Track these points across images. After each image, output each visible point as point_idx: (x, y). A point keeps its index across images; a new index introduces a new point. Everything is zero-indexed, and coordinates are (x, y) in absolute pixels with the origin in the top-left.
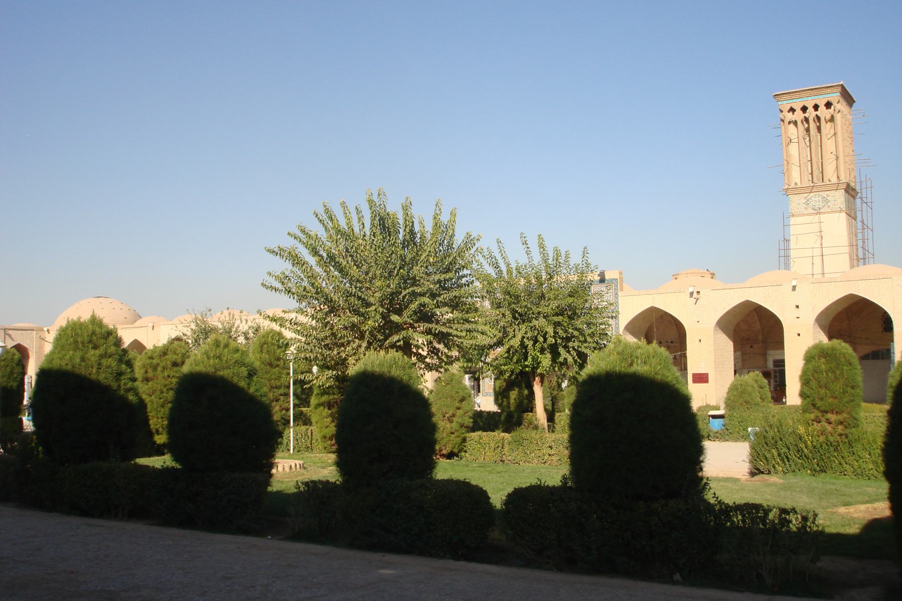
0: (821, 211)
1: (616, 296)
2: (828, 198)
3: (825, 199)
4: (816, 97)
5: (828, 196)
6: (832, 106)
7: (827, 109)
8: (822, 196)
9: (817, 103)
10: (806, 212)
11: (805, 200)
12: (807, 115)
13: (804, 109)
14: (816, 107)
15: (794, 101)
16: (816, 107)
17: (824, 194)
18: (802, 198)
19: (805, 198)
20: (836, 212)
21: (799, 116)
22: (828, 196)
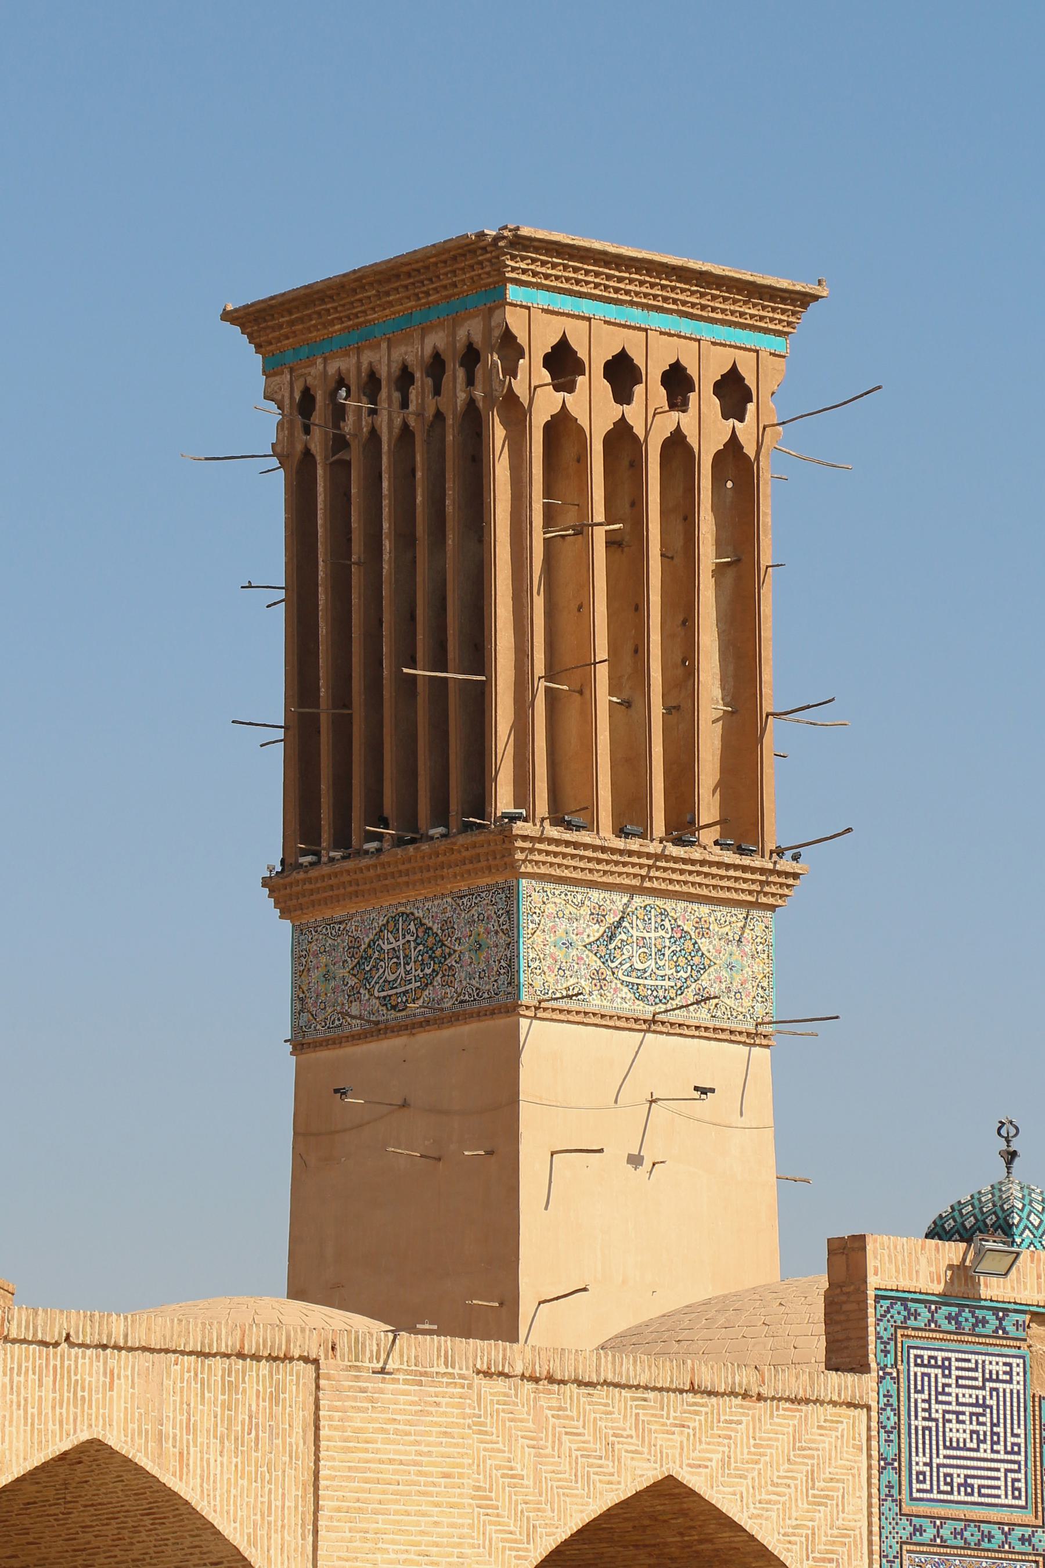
2: (704, 944)
3: (689, 945)
4: (686, 327)
6: (751, 407)
7: (726, 417)
9: (683, 362)
10: (595, 1002)
11: (596, 931)
15: (586, 307)
18: (585, 911)
19: (598, 917)
20: (731, 1036)
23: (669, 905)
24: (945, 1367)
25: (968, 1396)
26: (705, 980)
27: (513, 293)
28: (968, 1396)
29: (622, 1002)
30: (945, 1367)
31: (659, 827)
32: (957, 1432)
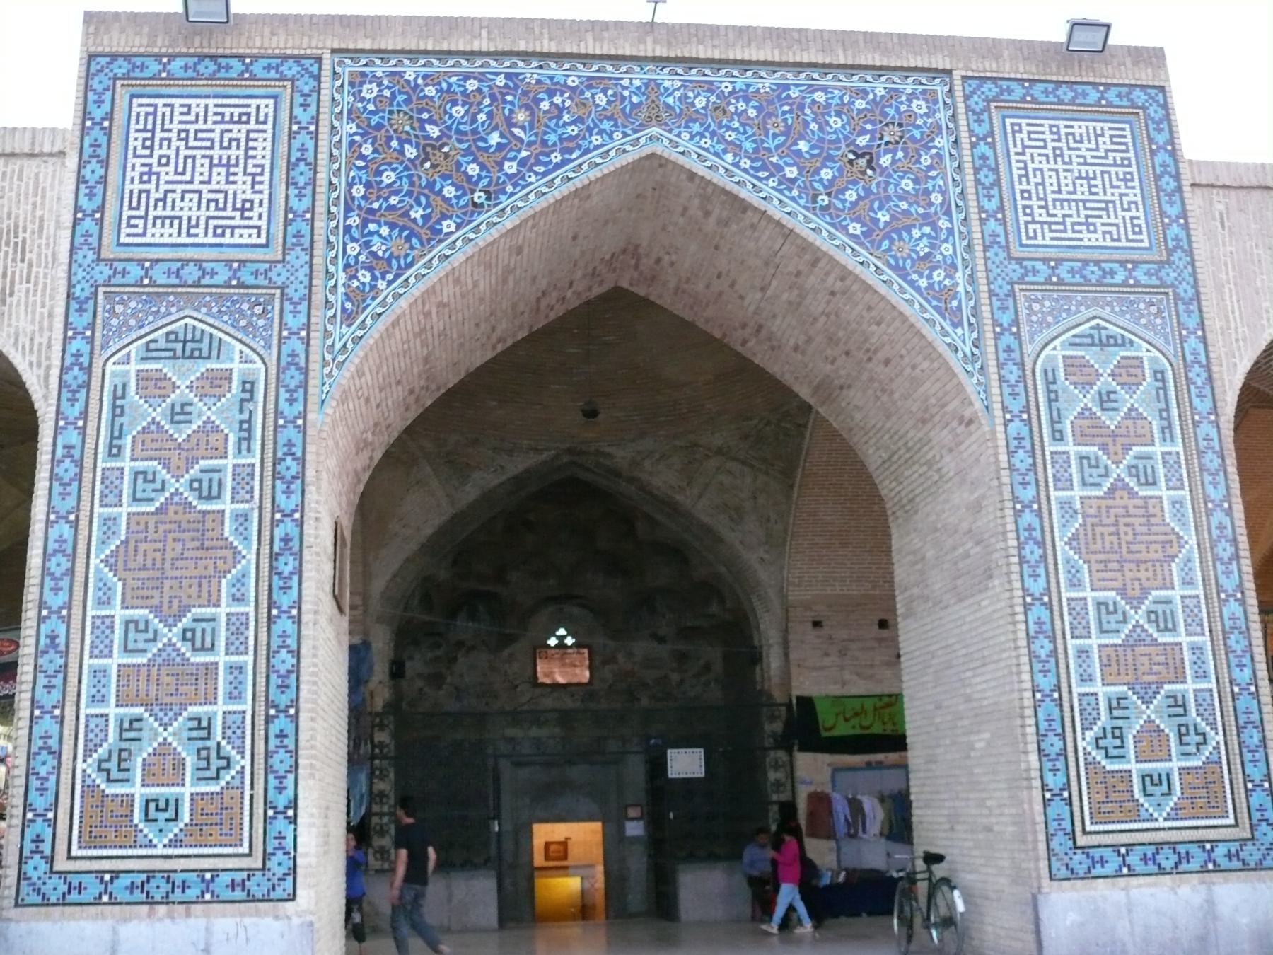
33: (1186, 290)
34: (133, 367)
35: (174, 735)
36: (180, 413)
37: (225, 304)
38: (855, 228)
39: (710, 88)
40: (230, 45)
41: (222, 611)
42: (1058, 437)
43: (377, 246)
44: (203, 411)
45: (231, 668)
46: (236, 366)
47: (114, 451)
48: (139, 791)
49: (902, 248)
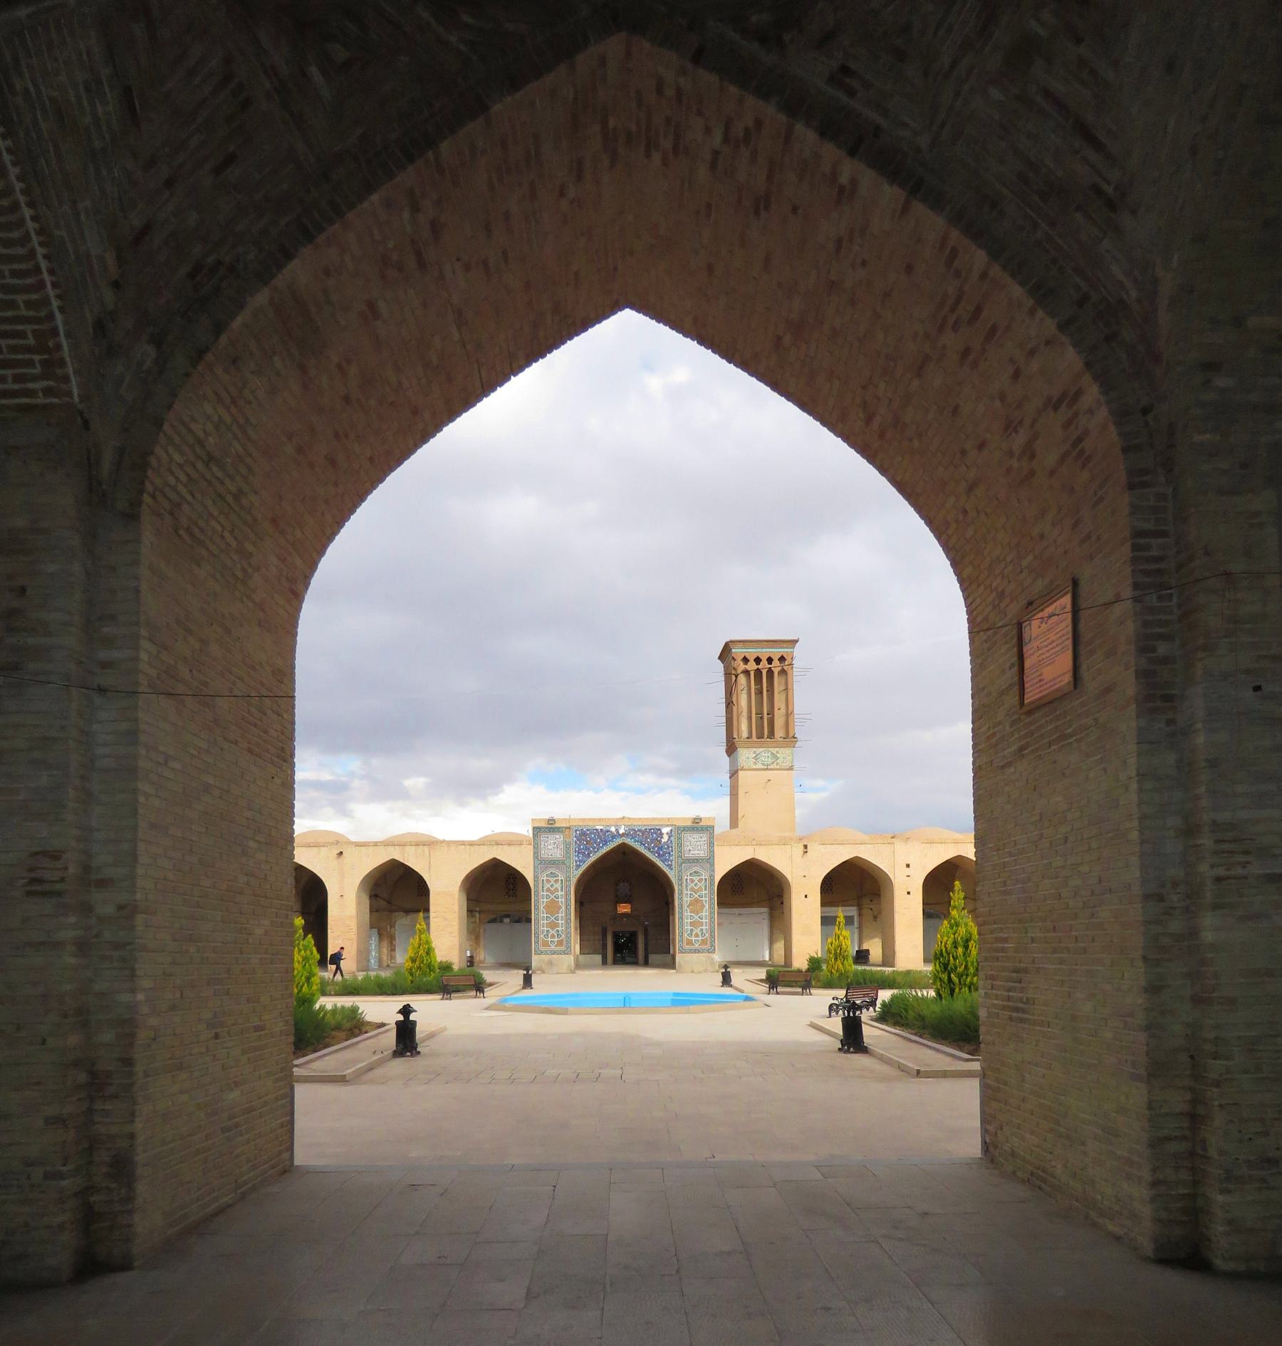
0: (769, 767)
1: (712, 845)
5: (777, 752)
8: (771, 753)
10: (754, 767)
12: (760, 667)
13: (758, 660)
14: (770, 660)
16: (770, 660)
17: (774, 750)
19: (755, 752)
20: (784, 769)
21: (752, 666)
22: (777, 752)
23: (770, 749)
24: (548, 837)
25: (552, 842)
26: (778, 761)
27: (733, 650)
28: (552, 842)
29: (760, 766)
30: (548, 837)
31: (766, 736)
32: (549, 847)
33: (712, 864)
34: (545, 879)
35: (554, 932)
36: (552, 886)
37: (558, 868)
38: (657, 855)
39: (634, 830)
40: (557, 825)
41: (560, 915)
42: (687, 890)
43: (580, 858)
44: (555, 886)
45: (562, 923)
46: (560, 879)
47: (543, 891)
48: (550, 940)
49: (664, 858)
